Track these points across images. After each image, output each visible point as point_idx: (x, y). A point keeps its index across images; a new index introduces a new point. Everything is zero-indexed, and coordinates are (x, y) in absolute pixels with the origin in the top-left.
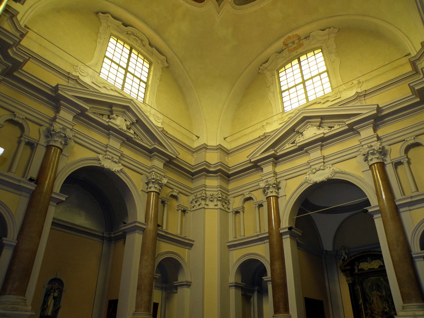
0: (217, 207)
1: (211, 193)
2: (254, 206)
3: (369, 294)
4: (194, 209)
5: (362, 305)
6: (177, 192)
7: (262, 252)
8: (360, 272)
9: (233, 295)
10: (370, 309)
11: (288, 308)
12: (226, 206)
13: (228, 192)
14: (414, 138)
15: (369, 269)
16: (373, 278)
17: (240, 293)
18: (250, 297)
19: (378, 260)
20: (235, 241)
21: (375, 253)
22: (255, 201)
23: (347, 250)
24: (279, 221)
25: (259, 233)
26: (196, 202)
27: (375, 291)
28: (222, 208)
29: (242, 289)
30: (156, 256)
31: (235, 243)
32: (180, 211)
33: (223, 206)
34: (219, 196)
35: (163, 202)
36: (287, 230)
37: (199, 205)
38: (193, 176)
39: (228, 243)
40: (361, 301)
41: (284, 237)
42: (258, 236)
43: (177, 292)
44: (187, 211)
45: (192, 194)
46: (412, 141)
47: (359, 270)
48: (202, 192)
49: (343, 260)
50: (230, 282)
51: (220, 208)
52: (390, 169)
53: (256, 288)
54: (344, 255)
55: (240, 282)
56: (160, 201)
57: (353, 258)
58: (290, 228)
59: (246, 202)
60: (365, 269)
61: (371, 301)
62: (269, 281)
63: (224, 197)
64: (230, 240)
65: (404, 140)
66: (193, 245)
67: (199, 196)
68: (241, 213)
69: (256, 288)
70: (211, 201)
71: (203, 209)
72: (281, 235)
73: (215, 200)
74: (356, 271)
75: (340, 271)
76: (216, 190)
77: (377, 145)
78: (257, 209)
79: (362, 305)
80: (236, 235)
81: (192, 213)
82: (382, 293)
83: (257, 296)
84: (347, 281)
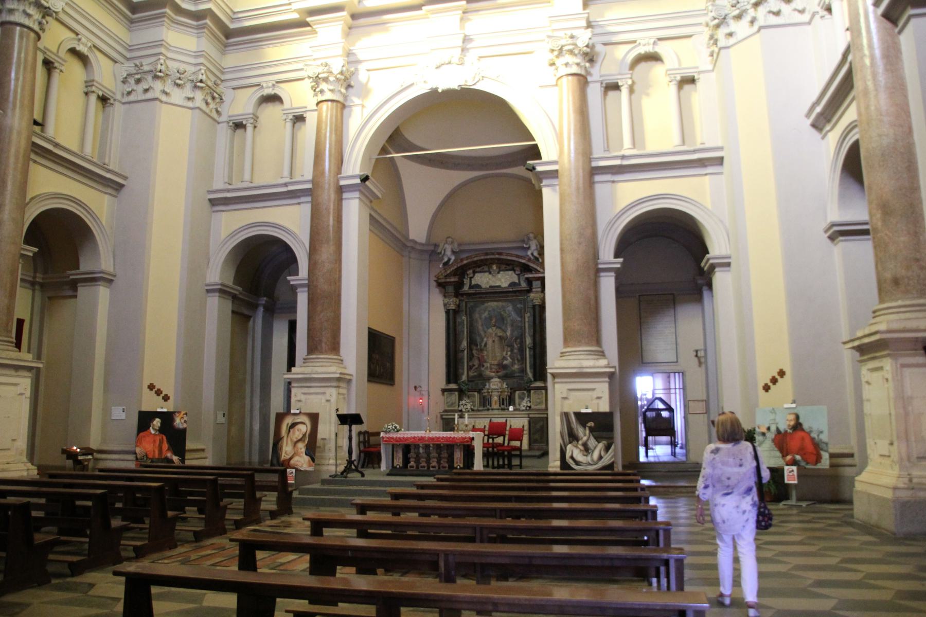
0: (190, 104)
1: (182, 67)
2: (285, 117)
3: (482, 333)
4: (132, 98)
6: (89, 44)
7: (291, 223)
8: (472, 291)
9: (216, 311)
11: (339, 343)
12: (212, 105)
13: (223, 73)
14: (654, 43)
15: (491, 287)
16: (494, 304)
17: (228, 305)
18: (248, 318)
19: (510, 272)
20: (228, 191)
21: (509, 258)
22: (287, 104)
23: (456, 245)
24: (340, 161)
25: (288, 180)
26: (138, 81)
28: (204, 107)
29: (234, 297)
30: (27, 200)
31: (229, 195)
32: (93, 98)
33: (207, 104)
34: (200, 77)
35: (48, 64)
36: (358, 181)
37: (146, 91)
38: (133, 13)
39: (210, 192)
40: (464, 344)
41: (345, 195)
42: (286, 185)
43: (76, 297)
44: (112, 101)
45: (128, 59)
46: (649, 49)
47: (471, 287)
48: (157, 58)
49: (446, 264)
50: (208, 281)
51: (198, 108)
52: (594, 92)
53: (263, 300)
54: (449, 253)
55: (230, 283)
56: (40, 58)
57: (465, 262)
58: (365, 179)
59: (264, 105)
60: (483, 286)
62: (302, 286)
63: (210, 84)
64: (215, 187)
65: (635, 42)
66: (122, 186)
67: (146, 68)
68: (250, 128)
69: (263, 300)
70: (178, 85)
71: (158, 102)
72: (341, 190)
73: (189, 86)
74: (466, 288)
75: (435, 284)
76: (193, 61)
77: (584, 38)
78: (289, 125)
80: (230, 177)
81: (123, 107)
82: (505, 332)
83: (264, 317)
84: (445, 305)
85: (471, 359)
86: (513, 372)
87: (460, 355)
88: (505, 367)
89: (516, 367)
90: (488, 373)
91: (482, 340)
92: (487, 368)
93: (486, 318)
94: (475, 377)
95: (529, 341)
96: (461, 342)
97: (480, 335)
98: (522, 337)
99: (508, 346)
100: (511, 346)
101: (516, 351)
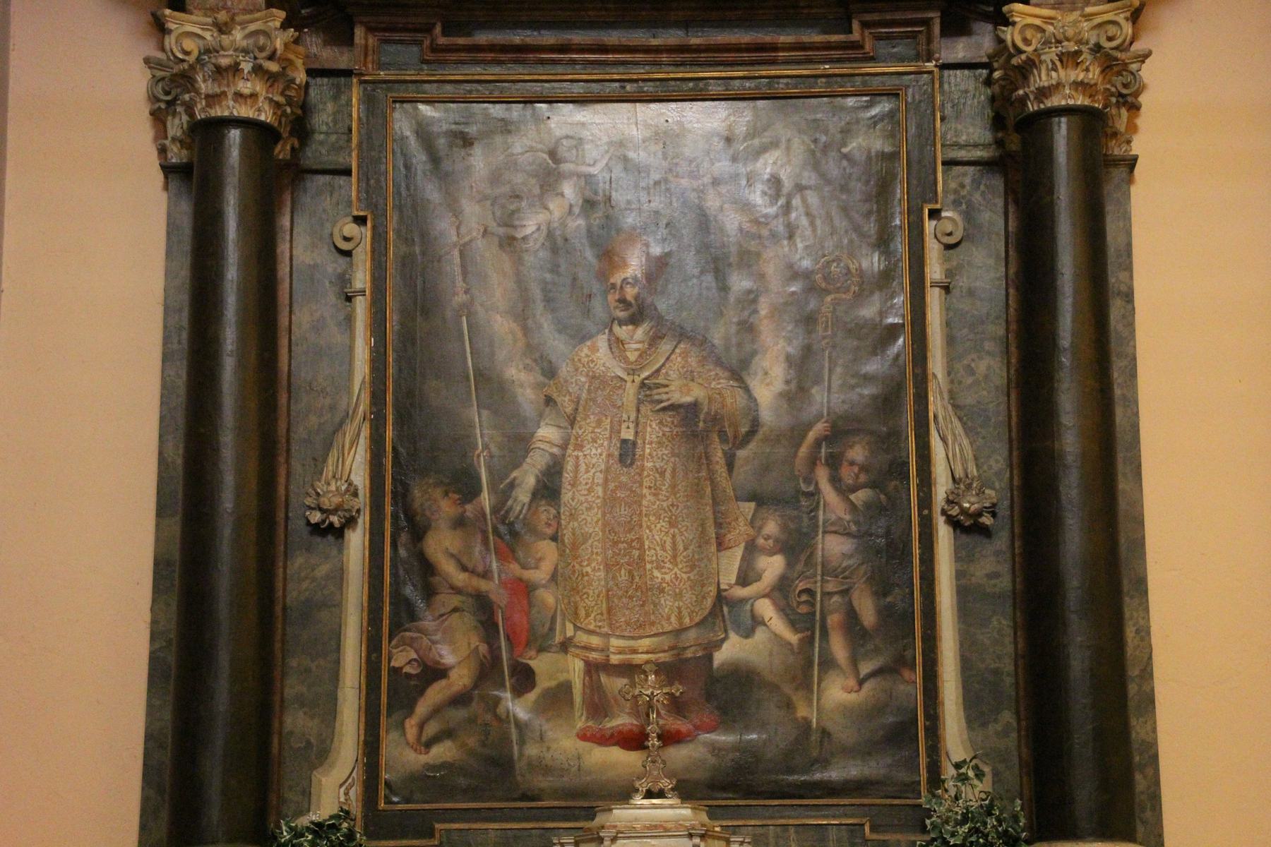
3: (521, 379)
5: (357, 540)
10: (483, 607)
27: (636, 337)
40: (354, 465)
61: (528, 477)
79: (357, 540)
82: (738, 373)
85: (405, 615)
86: (810, 743)
87: (301, 571)
88: (731, 693)
89: (838, 693)
90: (565, 746)
91: (520, 443)
92: (558, 698)
93: (556, 244)
94: (432, 783)
95: (959, 459)
96: (328, 441)
97: (492, 387)
98: (892, 420)
99: (760, 500)
100: (787, 499)
101: (835, 547)
